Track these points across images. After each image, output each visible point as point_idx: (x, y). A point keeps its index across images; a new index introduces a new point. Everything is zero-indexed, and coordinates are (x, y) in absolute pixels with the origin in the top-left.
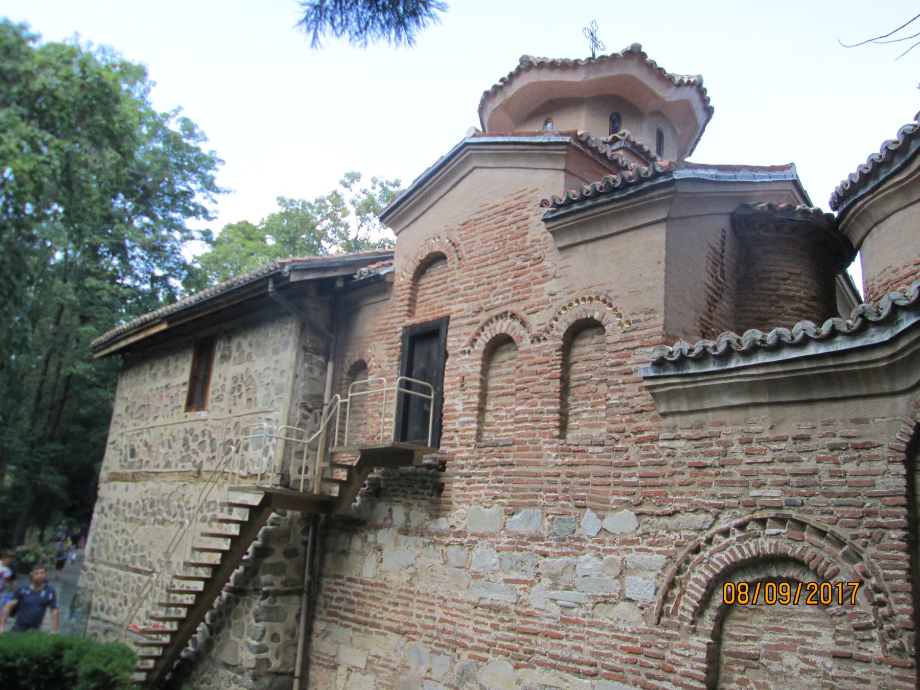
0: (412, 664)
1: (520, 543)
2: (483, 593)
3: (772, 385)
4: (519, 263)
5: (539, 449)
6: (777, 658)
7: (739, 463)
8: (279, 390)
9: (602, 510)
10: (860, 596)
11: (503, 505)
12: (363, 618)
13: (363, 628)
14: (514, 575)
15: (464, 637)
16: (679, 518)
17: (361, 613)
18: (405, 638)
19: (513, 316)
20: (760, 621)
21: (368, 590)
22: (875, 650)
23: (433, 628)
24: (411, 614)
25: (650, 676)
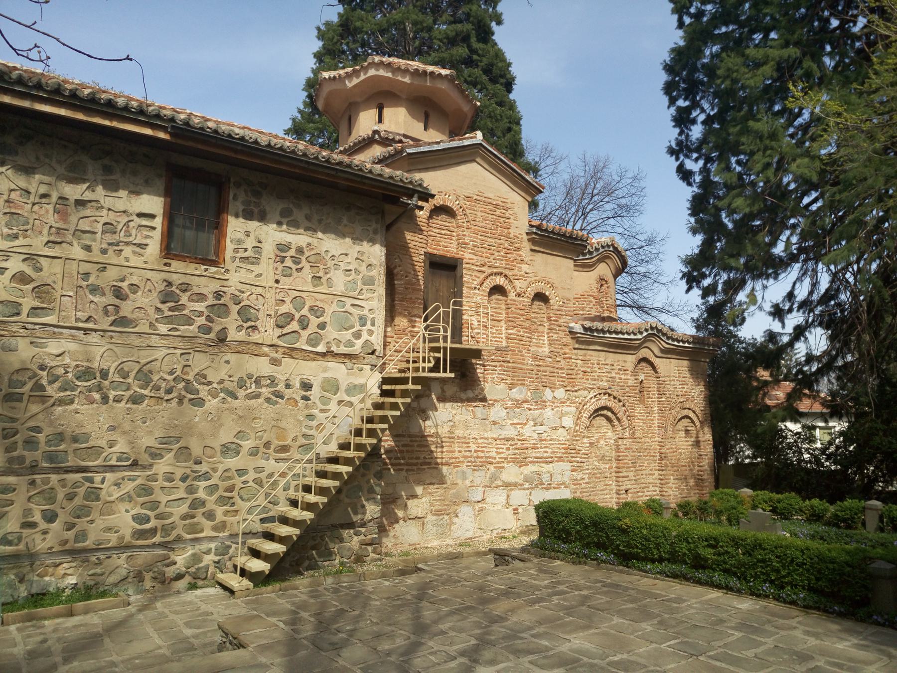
0: (459, 482)
1: (518, 404)
2: (500, 432)
3: (610, 345)
4: (506, 245)
5: (523, 356)
6: (598, 442)
7: (596, 372)
8: (369, 281)
9: (553, 388)
10: (625, 419)
11: (507, 384)
12: (415, 461)
13: (415, 468)
14: (515, 421)
15: (491, 457)
16: (580, 392)
17: (412, 458)
18: (452, 467)
19: (506, 276)
20: (593, 430)
21: (416, 441)
22: (627, 434)
23: (471, 456)
24: (454, 451)
25: (572, 457)
